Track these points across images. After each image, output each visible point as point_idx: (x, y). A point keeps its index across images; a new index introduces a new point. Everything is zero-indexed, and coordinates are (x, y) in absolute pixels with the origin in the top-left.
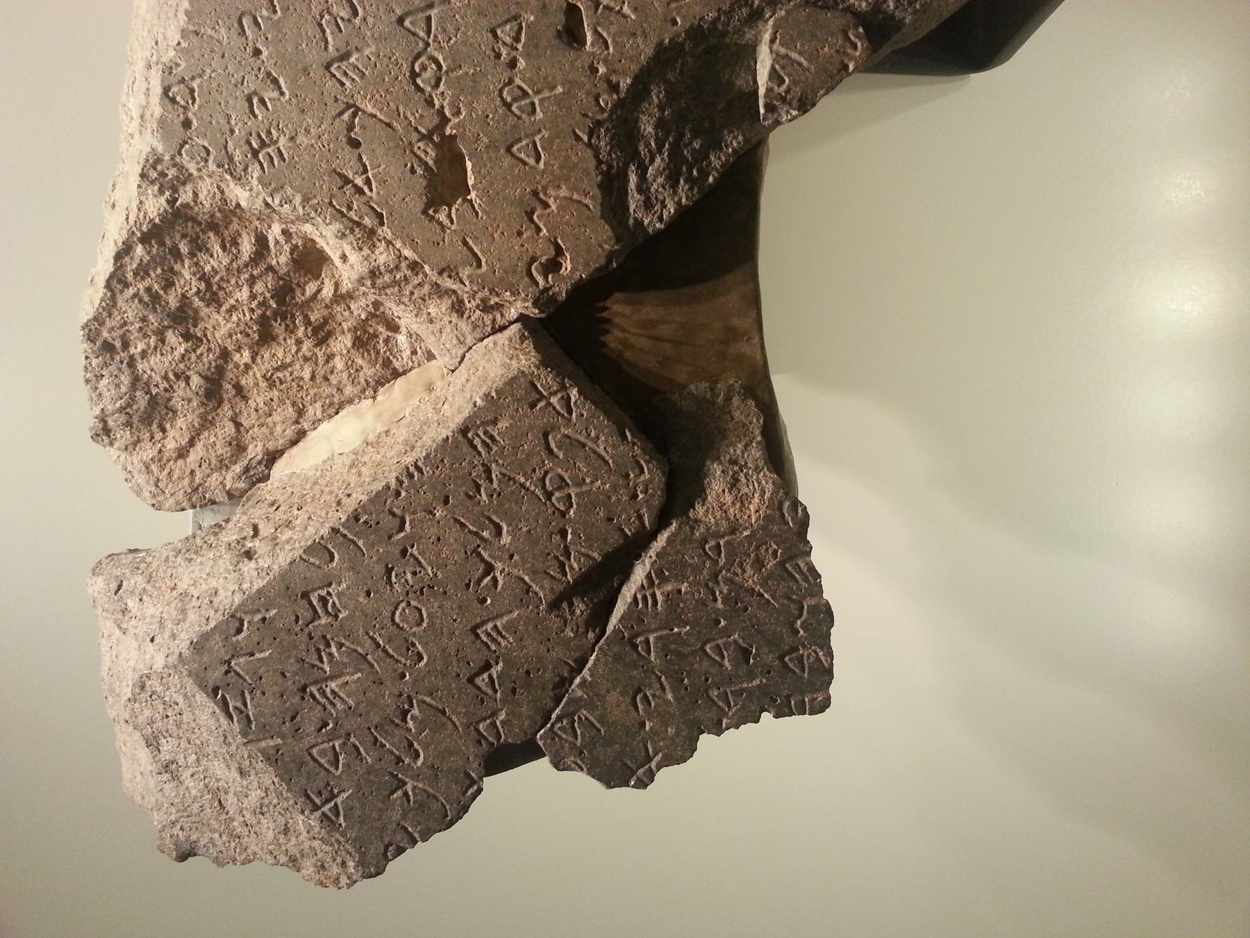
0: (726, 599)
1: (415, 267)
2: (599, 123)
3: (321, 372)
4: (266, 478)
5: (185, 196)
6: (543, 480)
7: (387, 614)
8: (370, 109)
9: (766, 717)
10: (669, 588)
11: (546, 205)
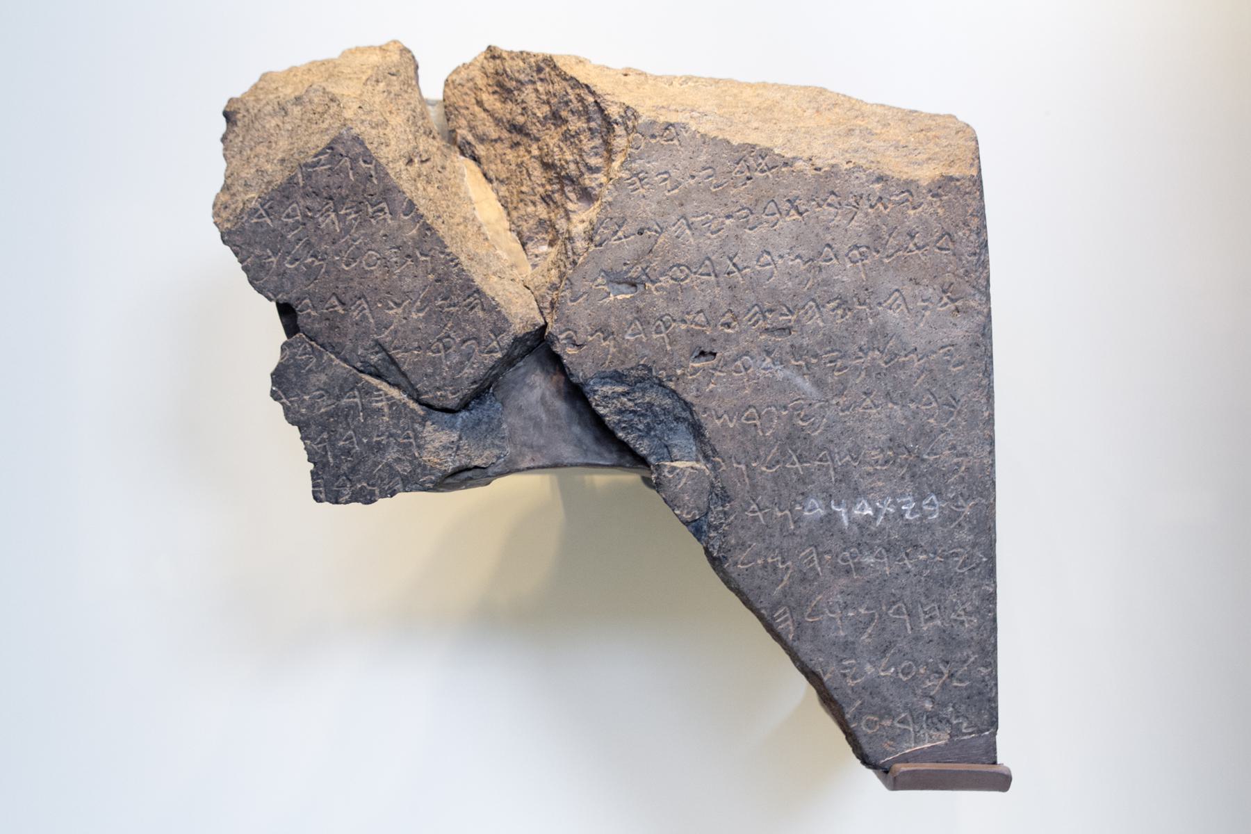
0: (379, 443)
1: (574, 263)
2: (650, 370)
3: (527, 198)
4: (463, 154)
5: (619, 130)
6: (449, 336)
7: (373, 246)
8: (660, 241)
9: (311, 466)
10: (386, 410)
11: (605, 339)
